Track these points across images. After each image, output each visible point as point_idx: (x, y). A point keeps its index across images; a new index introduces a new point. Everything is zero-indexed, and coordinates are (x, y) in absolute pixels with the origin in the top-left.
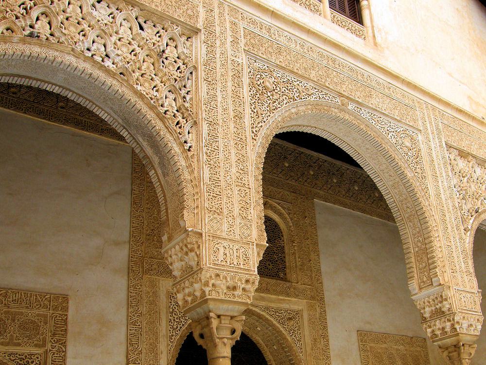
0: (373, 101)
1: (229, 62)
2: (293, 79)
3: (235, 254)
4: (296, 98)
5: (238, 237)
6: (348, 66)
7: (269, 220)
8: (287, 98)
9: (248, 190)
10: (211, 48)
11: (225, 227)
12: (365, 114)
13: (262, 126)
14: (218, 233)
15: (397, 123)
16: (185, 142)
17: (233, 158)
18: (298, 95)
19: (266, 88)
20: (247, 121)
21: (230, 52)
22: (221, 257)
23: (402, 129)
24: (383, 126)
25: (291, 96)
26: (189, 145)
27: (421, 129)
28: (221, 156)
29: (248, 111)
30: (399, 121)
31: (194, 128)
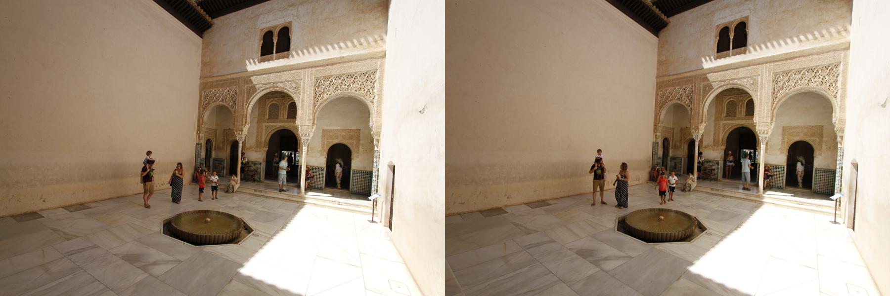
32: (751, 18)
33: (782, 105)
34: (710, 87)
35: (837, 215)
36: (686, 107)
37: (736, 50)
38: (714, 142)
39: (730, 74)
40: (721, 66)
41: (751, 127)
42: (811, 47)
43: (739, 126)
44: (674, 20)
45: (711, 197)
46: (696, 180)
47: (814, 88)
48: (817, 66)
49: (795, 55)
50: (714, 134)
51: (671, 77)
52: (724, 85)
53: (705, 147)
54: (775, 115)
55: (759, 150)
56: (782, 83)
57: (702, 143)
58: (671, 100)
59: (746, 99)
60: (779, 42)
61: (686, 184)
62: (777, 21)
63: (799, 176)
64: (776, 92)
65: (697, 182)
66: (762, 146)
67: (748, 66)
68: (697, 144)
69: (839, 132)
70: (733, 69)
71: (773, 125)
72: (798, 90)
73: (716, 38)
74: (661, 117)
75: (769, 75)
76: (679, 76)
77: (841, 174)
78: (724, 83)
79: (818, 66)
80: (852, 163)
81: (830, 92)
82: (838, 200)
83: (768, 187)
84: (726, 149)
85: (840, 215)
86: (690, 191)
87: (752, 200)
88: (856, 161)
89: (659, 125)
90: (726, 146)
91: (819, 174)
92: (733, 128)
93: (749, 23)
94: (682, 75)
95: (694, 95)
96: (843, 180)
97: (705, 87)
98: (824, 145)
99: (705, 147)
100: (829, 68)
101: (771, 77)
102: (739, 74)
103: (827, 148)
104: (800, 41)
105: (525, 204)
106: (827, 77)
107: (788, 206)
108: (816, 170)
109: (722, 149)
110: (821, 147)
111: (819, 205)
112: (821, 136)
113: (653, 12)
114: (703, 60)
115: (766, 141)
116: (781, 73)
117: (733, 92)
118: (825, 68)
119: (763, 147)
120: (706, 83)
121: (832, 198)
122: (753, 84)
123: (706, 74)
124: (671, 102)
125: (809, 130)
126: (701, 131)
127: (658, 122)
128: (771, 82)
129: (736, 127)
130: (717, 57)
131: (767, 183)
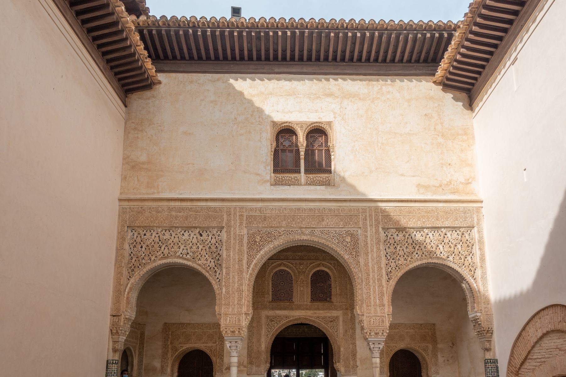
0: (324, 223)
1: (237, 236)
2: (272, 231)
3: (234, 319)
4: (273, 240)
5: (236, 312)
6: (309, 208)
7: (323, 272)
8: (267, 242)
9: (242, 292)
10: (228, 232)
13: (252, 261)
14: (227, 313)
15: (341, 229)
16: (218, 278)
17: (236, 280)
18: (274, 238)
19: (256, 242)
20: (245, 262)
21: (238, 231)
22: (228, 321)
23: (344, 232)
24: (330, 235)
25: (270, 240)
26: (219, 279)
27: (361, 226)
28: (231, 281)
29: (246, 256)
30: (342, 228)
31: (221, 272)
37: (311, 176)
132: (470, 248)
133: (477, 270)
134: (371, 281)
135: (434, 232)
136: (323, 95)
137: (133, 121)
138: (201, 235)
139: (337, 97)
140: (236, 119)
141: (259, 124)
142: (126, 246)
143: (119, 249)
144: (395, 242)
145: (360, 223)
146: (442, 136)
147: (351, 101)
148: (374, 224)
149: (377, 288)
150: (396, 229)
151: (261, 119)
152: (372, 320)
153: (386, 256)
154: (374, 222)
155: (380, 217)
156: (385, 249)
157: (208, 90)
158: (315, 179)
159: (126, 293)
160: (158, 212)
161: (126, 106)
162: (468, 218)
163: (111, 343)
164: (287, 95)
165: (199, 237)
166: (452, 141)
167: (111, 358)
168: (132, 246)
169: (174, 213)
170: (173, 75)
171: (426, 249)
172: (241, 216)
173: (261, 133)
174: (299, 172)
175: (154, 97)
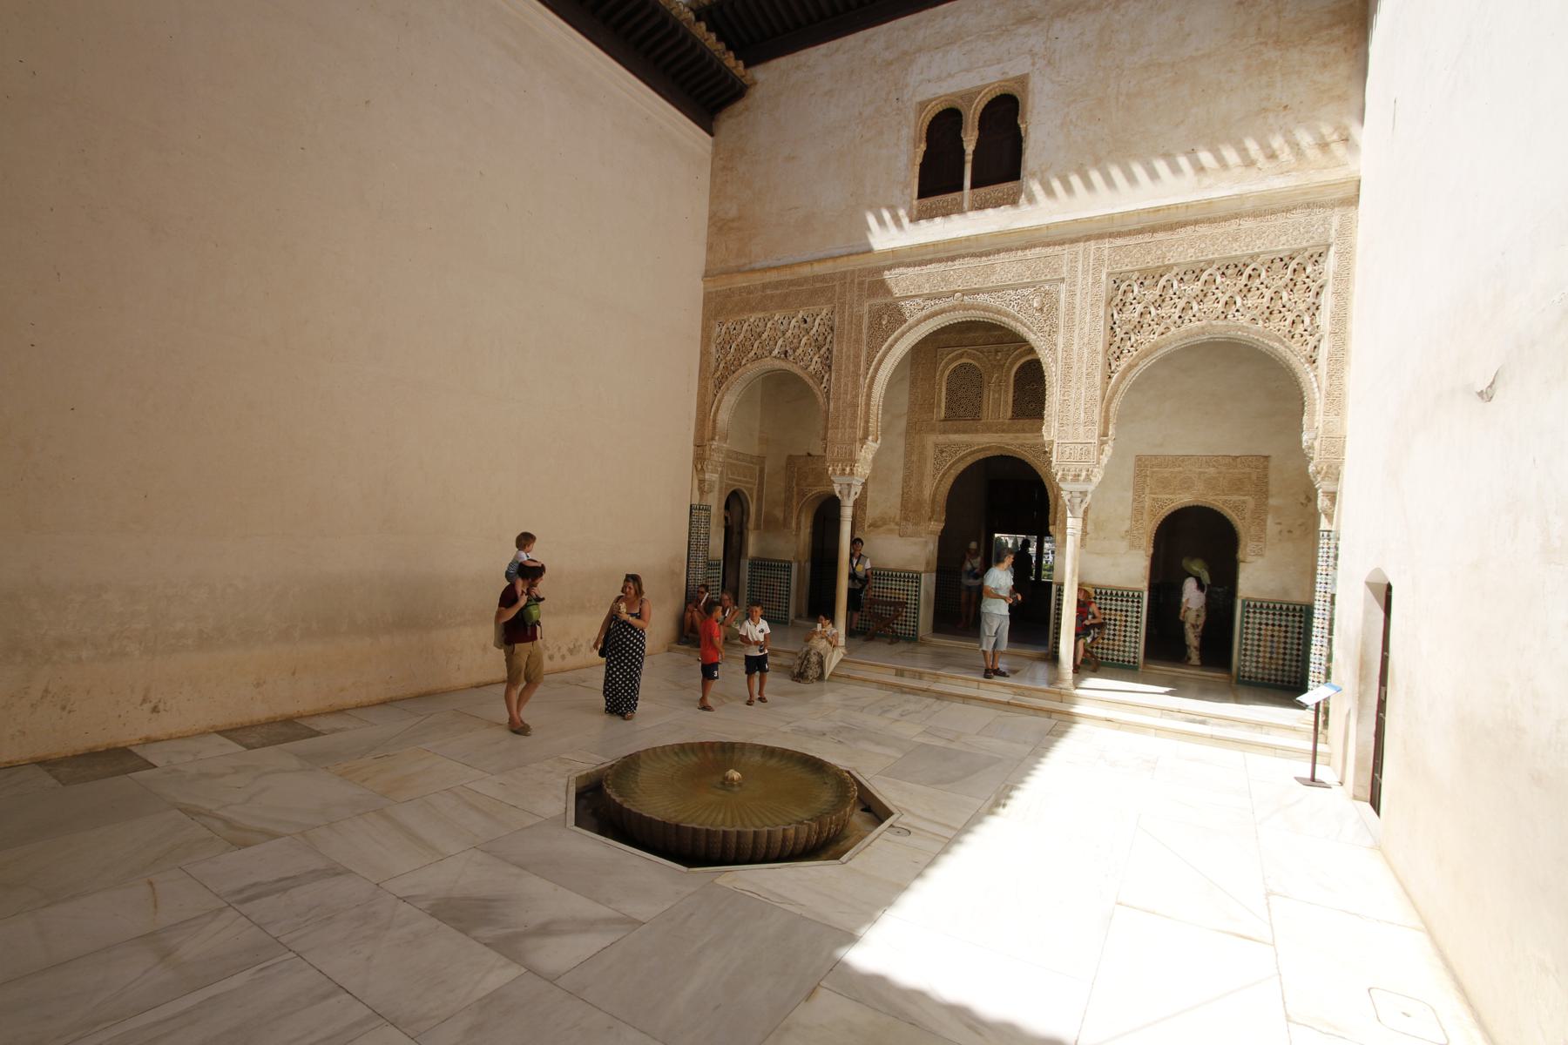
11: (840, 435)
12: (982, 298)
20: (863, 358)
22: (835, 454)
27: (1064, 275)
32: (1035, 83)
33: (1136, 386)
34: (897, 317)
35: (1318, 758)
36: (810, 382)
37: (982, 191)
38: (904, 506)
39: (961, 274)
40: (935, 244)
41: (1030, 458)
42: (1236, 190)
43: (989, 454)
44: (768, 77)
45: (897, 699)
46: (842, 640)
47: (1241, 328)
48: (1253, 257)
49: (1181, 217)
50: (906, 480)
51: (757, 276)
52: (943, 311)
53: (874, 525)
54: (1113, 420)
55: (1058, 537)
56: (1139, 308)
57: (864, 511)
58: (757, 358)
59: (1012, 364)
60: (1130, 169)
61: (808, 653)
62: (1122, 99)
63: (1187, 626)
64: (1117, 339)
65: (846, 646)
66: (1070, 522)
67: (1024, 248)
68: (847, 512)
69: (1323, 479)
70: (974, 255)
71: (1108, 449)
72: (1189, 335)
73: (916, 147)
74: (719, 417)
75: (1096, 282)
76: (786, 275)
77: (1331, 621)
78: (942, 304)
79: (1258, 255)
80: (1368, 584)
81: (1295, 345)
82: (1321, 706)
83: (1089, 664)
84: (942, 531)
85: (1329, 755)
86: (821, 677)
87: (1037, 710)
88: (1384, 575)
89: (715, 444)
90: (947, 521)
91: (1255, 619)
92: (970, 461)
93: (1030, 102)
94: (796, 269)
95: (840, 343)
96: (1335, 638)
97: (877, 315)
98: (1270, 521)
99: (874, 525)
100: (1293, 265)
101: (1103, 287)
102: (993, 273)
103: (1281, 532)
104: (1200, 169)
105: (220, 733)
106: (1285, 295)
107: (1158, 730)
108: (1246, 605)
109: (932, 533)
110: (1263, 530)
111: (1259, 725)
112: (1262, 489)
113: (696, 43)
114: (871, 220)
115: (1084, 506)
116: (1137, 274)
117: (971, 335)
118: (1278, 264)
119: (1073, 524)
120: (880, 301)
121: (1303, 698)
122: (1041, 309)
123: (880, 270)
124: (756, 364)
125: (1223, 469)
126: (863, 469)
127: (708, 434)
128: (1103, 305)
129: (981, 456)
130: (919, 211)
131: (1086, 651)
132: (1311, 293)
133: (1322, 341)
134: (1074, 380)
135: (1227, 268)
136: (1013, 24)
137: (721, 156)
138: (805, 322)
139: (1041, 20)
140: (860, 114)
141: (897, 114)
142: (713, 350)
143: (705, 353)
144: (1135, 299)
145: (1065, 269)
146: (1276, 42)
147: (1070, 19)
148: (1091, 268)
149: (1083, 390)
150: (1139, 271)
151: (900, 103)
152: (1068, 450)
153: (1112, 328)
154: (1091, 264)
155: (1106, 252)
156: (1112, 315)
157: (822, 74)
158: (988, 196)
159: (712, 414)
160: (749, 293)
161: (712, 135)
162: (1316, 227)
163: (696, 482)
164: (947, 44)
165: (803, 325)
166: (1301, 50)
167: (696, 502)
168: (719, 347)
169: (769, 292)
170: (774, 63)
171: (1201, 307)
172: (861, 283)
173: (899, 130)
174: (960, 188)
175: (747, 109)
